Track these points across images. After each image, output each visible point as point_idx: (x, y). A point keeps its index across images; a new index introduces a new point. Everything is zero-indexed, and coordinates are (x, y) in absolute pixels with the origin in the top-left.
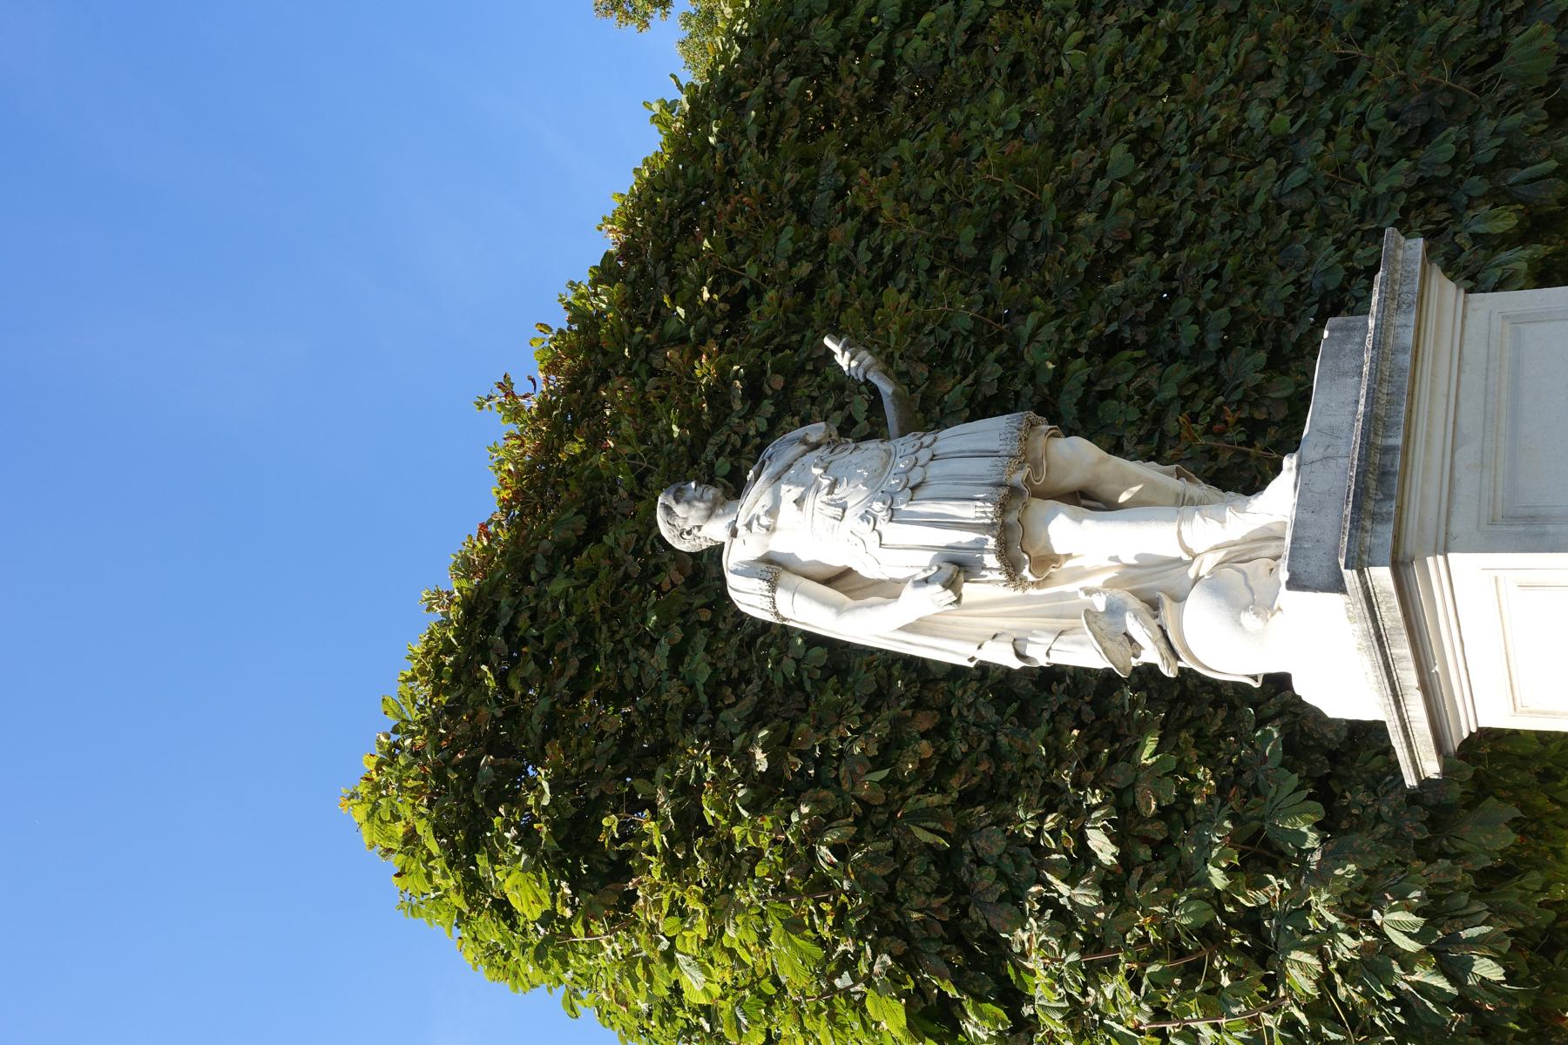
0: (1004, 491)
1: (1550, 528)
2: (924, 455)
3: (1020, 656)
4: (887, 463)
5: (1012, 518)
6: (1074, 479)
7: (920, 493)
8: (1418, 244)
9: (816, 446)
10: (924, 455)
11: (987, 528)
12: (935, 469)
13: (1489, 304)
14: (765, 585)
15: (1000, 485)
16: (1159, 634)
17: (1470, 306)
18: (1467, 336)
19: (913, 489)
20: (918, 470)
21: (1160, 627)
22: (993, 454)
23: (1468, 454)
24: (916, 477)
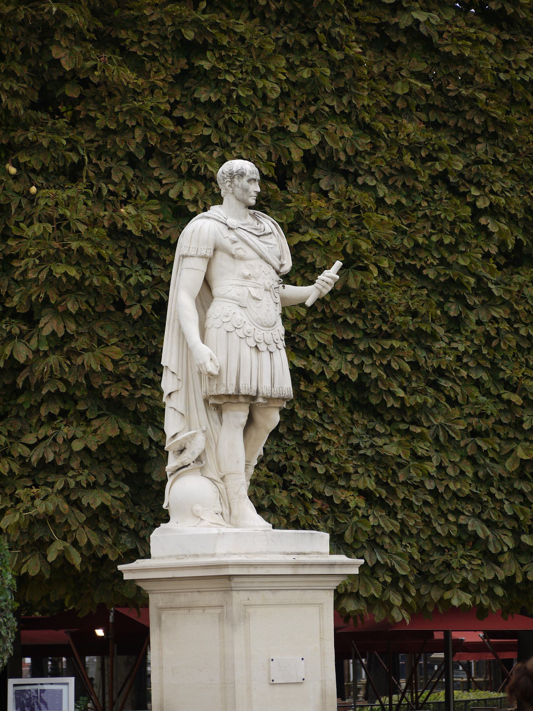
2: (273, 348)
3: (170, 395)
5: (242, 399)
6: (259, 417)
7: (254, 351)
8: (356, 571)
10: (273, 348)
11: (238, 389)
12: (266, 356)
13: (329, 599)
15: (257, 392)
18: (316, 591)
19: (256, 347)
21: (189, 464)
22: (273, 385)
23: (269, 595)
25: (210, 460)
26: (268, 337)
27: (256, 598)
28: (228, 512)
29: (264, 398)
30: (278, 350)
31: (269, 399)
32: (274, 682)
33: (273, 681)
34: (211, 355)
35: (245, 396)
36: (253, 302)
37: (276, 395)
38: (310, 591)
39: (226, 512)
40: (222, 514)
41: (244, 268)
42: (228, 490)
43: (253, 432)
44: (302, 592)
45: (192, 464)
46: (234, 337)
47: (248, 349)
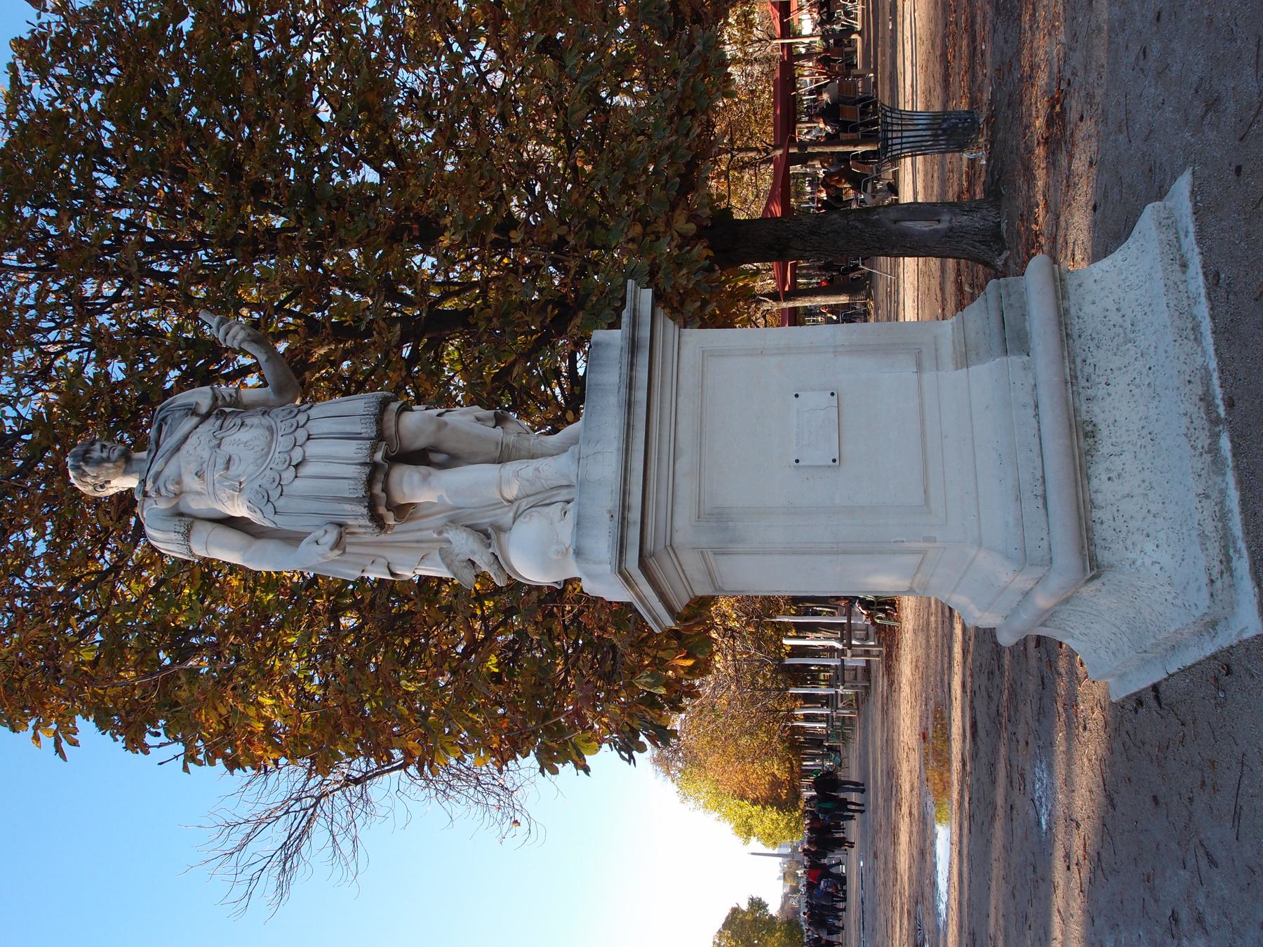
0: (367, 470)
1: (730, 524)
2: (301, 434)
3: (393, 574)
4: (272, 440)
6: (420, 443)
7: (304, 471)
8: (647, 295)
9: (205, 417)
11: (358, 500)
12: (313, 448)
14: (179, 537)
16: (492, 558)
17: (683, 339)
19: (296, 467)
20: (298, 451)
23: (684, 464)
24: (297, 455)
25: (484, 520)
26: (283, 443)
27: (686, 488)
28: (564, 491)
29: (374, 450)
30: (310, 423)
31: (380, 436)
32: (837, 457)
33: (834, 461)
34: (309, 543)
35: (370, 482)
36: (234, 470)
37: (370, 430)
38: (681, 377)
39: (564, 495)
40: (568, 502)
41: (191, 483)
42: (529, 492)
43: (451, 444)
44: (682, 393)
45: (491, 550)
46: (280, 504)
47: (298, 482)
